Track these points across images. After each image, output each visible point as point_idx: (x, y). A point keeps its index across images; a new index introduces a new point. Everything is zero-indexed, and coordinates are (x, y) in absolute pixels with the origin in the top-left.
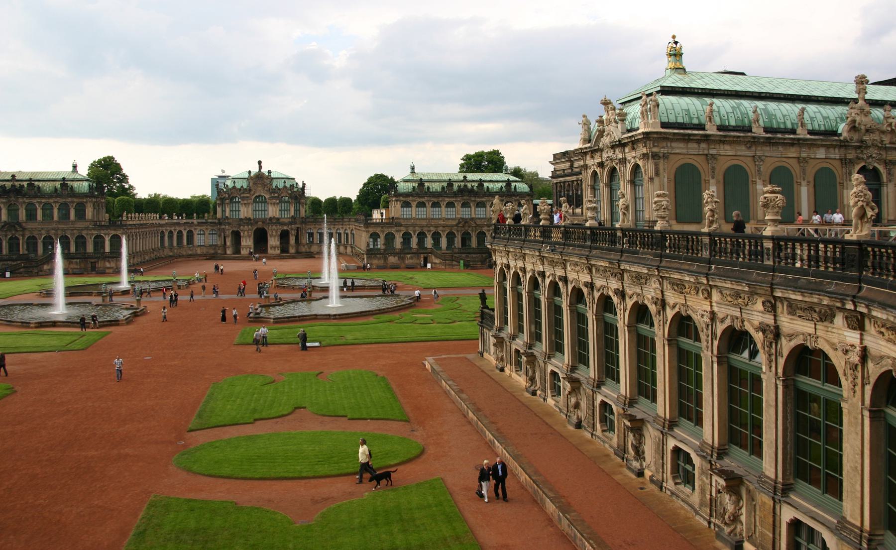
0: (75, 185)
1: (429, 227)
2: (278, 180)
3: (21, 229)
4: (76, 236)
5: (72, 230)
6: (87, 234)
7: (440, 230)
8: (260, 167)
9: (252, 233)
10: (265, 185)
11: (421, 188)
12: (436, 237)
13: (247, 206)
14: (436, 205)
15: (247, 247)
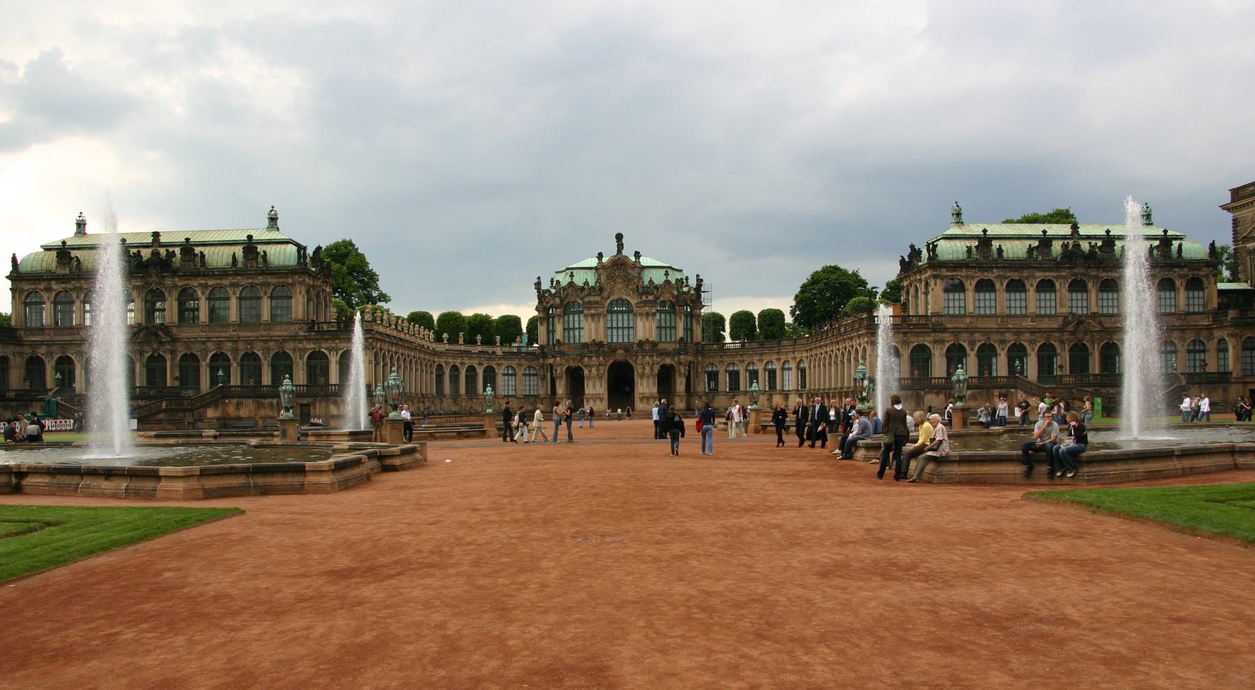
0: (272, 250)
1: (1003, 333)
2: (654, 271)
3: (168, 339)
4: (272, 353)
5: (266, 341)
6: (294, 350)
7: (1025, 339)
8: (620, 247)
9: (604, 371)
10: (629, 280)
11: (985, 250)
12: (1017, 352)
13: (596, 318)
14: (1016, 286)
15: (598, 397)
